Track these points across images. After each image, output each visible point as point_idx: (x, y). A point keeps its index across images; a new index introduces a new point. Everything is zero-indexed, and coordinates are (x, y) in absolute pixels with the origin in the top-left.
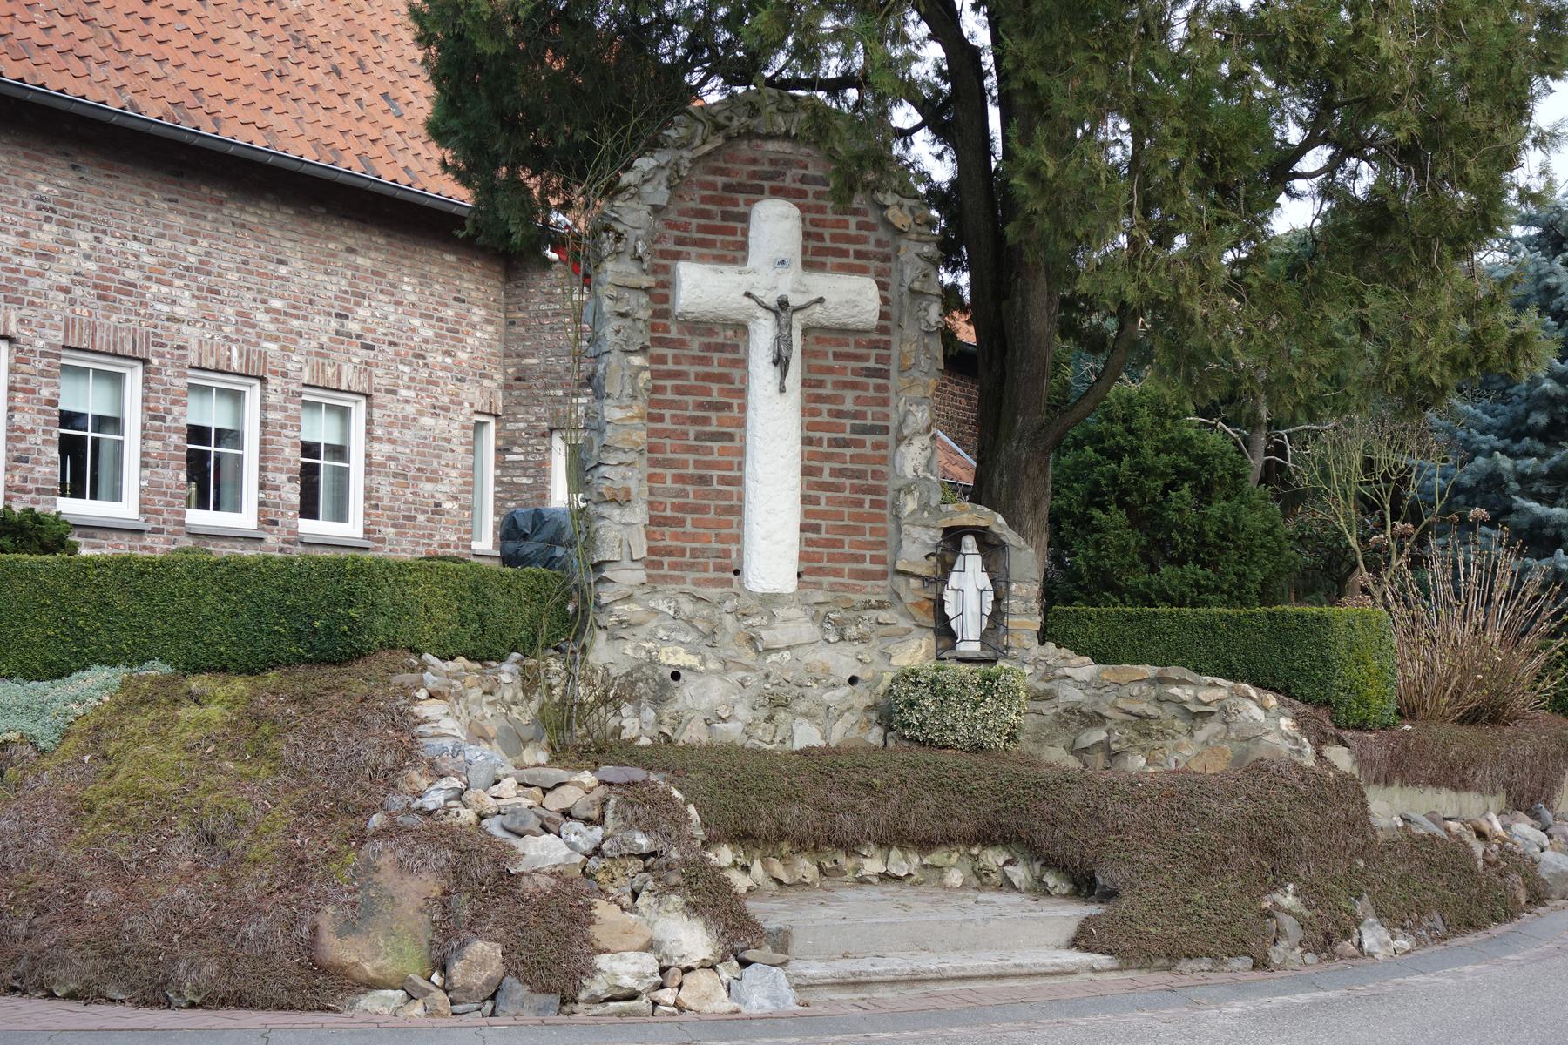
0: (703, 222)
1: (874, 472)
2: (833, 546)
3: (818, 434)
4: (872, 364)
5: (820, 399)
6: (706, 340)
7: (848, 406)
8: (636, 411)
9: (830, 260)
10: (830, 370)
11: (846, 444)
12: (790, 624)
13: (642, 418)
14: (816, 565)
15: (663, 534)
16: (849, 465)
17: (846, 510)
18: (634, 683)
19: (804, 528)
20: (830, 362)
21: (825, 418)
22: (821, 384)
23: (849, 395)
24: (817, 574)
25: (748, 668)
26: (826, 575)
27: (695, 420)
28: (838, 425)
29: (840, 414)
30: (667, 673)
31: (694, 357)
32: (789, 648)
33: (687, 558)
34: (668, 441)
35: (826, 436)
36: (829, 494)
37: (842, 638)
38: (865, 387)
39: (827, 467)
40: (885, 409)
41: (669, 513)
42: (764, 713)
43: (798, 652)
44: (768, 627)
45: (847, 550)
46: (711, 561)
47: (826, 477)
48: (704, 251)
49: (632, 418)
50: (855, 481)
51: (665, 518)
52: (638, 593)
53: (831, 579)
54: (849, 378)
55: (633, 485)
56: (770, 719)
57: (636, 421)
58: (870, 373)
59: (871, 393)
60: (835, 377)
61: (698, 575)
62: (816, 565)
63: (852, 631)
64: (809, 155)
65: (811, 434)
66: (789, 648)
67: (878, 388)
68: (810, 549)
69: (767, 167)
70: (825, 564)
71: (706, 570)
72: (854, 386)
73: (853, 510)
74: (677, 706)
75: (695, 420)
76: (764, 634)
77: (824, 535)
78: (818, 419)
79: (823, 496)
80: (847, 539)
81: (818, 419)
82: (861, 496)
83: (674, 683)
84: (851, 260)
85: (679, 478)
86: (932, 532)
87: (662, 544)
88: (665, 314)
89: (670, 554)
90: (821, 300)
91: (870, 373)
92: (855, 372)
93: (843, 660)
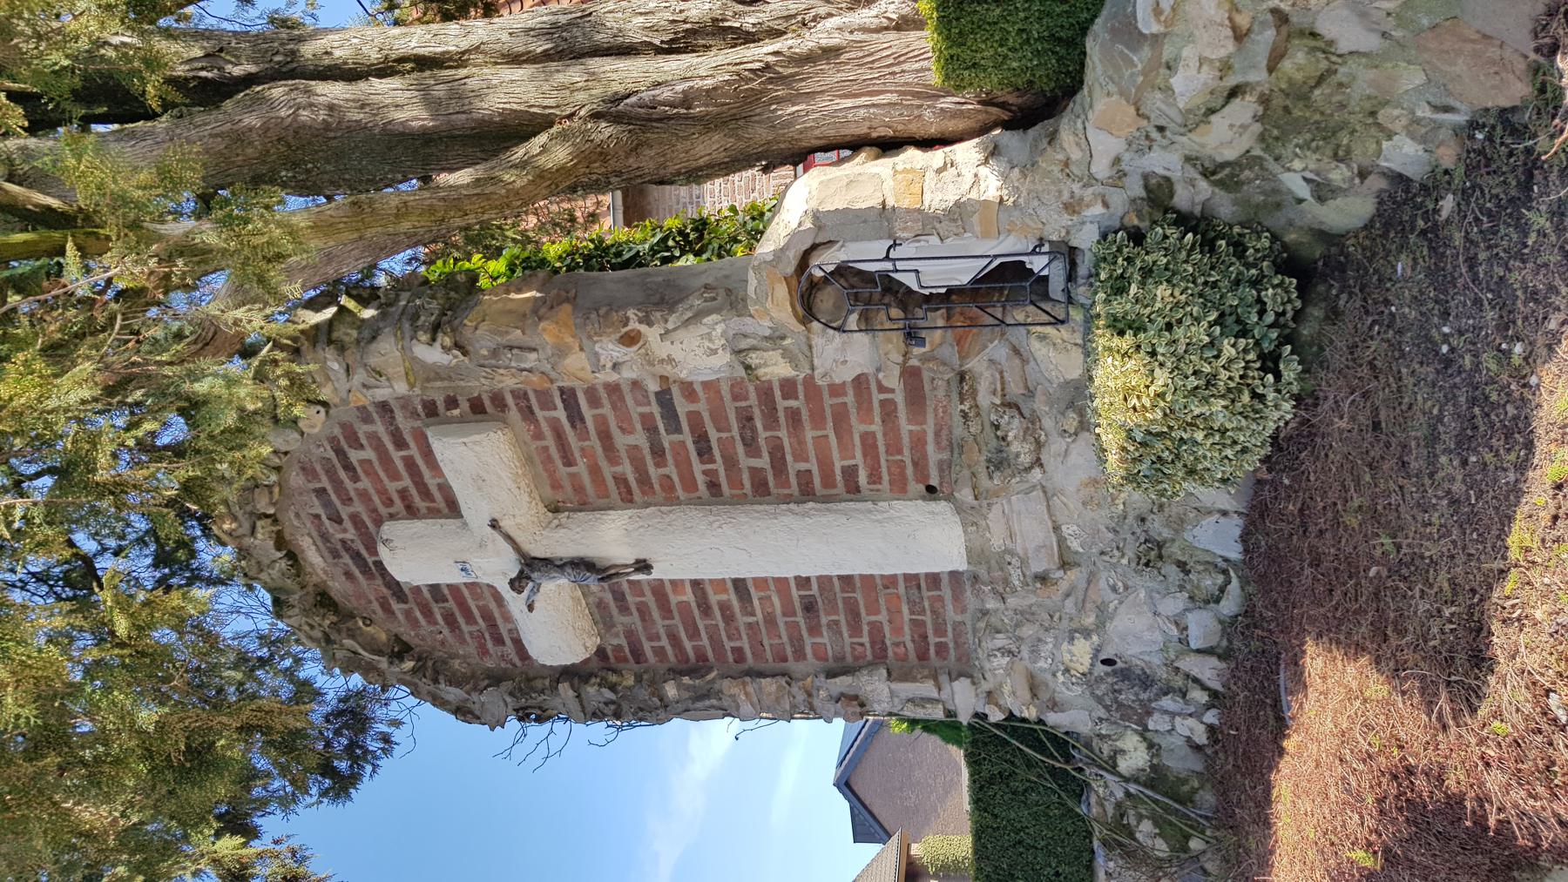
0: (461, 620)
1: (735, 398)
2: (875, 446)
3: (701, 479)
4: (561, 414)
5: (644, 480)
6: (615, 611)
7: (640, 439)
8: (735, 691)
9: (432, 482)
10: (595, 471)
11: (702, 440)
12: (1016, 527)
13: (744, 684)
14: (910, 471)
15: (897, 645)
16: (735, 432)
17: (810, 434)
18: (1120, 705)
19: (853, 490)
20: (581, 468)
21: (671, 469)
22: (621, 481)
23: (621, 441)
24: (926, 467)
25: (1091, 579)
26: (925, 456)
27: (729, 618)
28: (676, 455)
29: (658, 452)
30: (1101, 669)
31: (643, 620)
32: (1057, 529)
33: (928, 618)
34: (766, 643)
35: (698, 468)
36: (789, 458)
37: (1038, 462)
38: (602, 423)
39: (745, 462)
40: (626, 389)
41: (865, 639)
42: (1172, 570)
43: (1061, 519)
44: (1024, 562)
45: (876, 427)
46: (926, 594)
47: (764, 462)
48: (497, 615)
49: (747, 694)
50: (759, 425)
51: (873, 643)
52: (985, 686)
53: (930, 448)
54: (595, 442)
55: (835, 691)
56: (1182, 565)
57: (750, 689)
58: (575, 416)
59: (606, 410)
60: (603, 463)
61: (950, 607)
62: (910, 471)
63: (1021, 450)
64: (297, 515)
65: (702, 487)
66: (1057, 529)
67: (594, 401)
68: (886, 477)
69: (347, 559)
70: (907, 456)
71: (940, 599)
72: (605, 437)
73: (807, 425)
74: (1156, 660)
75: (729, 618)
76: (1037, 567)
77: (859, 459)
78: (676, 478)
79: (793, 467)
80: (858, 428)
81: (676, 478)
82: (781, 414)
83: (1120, 665)
84: (414, 451)
85: (814, 630)
86: (818, 341)
87: (910, 645)
88: (601, 652)
89: (925, 637)
90: (494, 524)
91: (575, 416)
92: (584, 436)
93: (1073, 458)
